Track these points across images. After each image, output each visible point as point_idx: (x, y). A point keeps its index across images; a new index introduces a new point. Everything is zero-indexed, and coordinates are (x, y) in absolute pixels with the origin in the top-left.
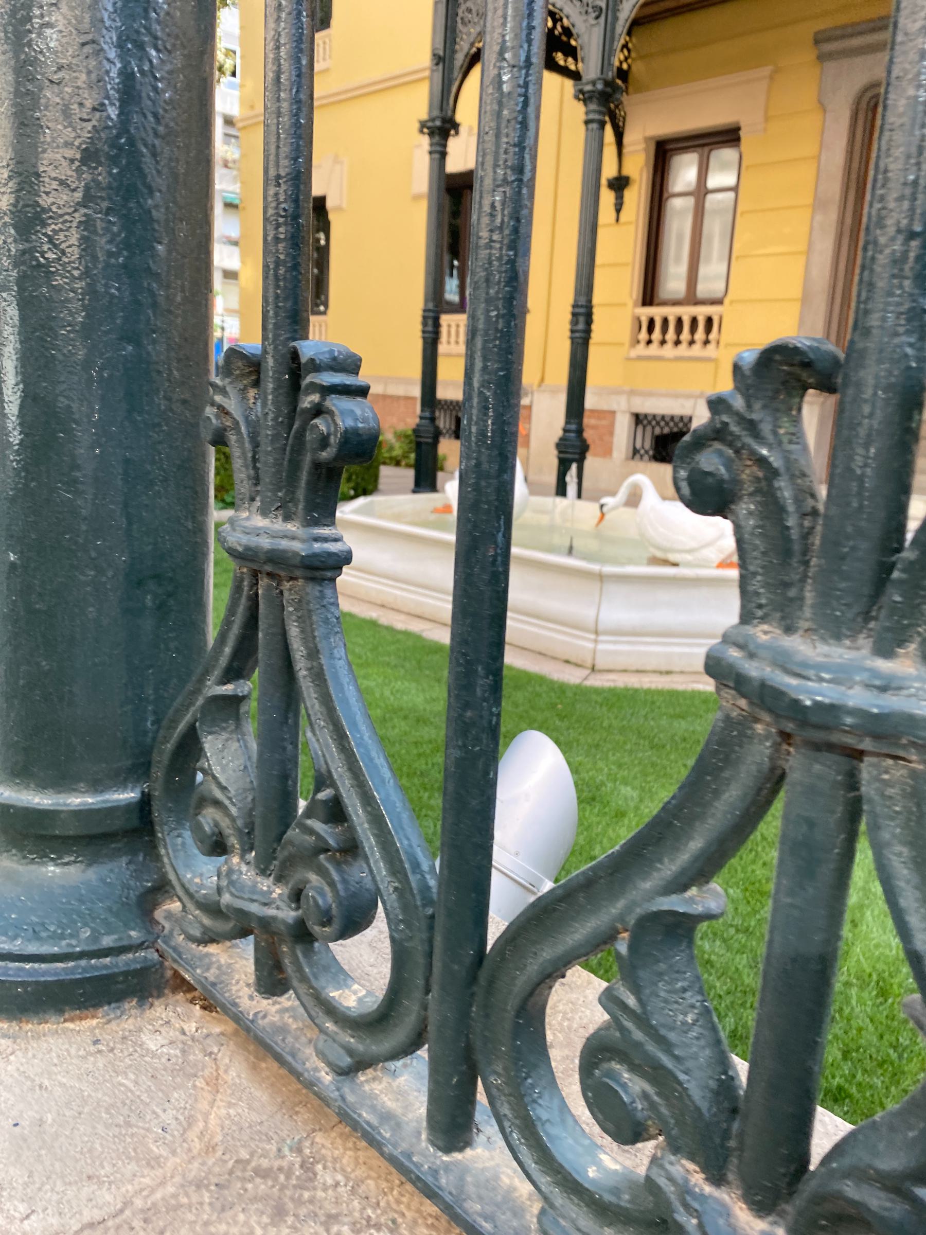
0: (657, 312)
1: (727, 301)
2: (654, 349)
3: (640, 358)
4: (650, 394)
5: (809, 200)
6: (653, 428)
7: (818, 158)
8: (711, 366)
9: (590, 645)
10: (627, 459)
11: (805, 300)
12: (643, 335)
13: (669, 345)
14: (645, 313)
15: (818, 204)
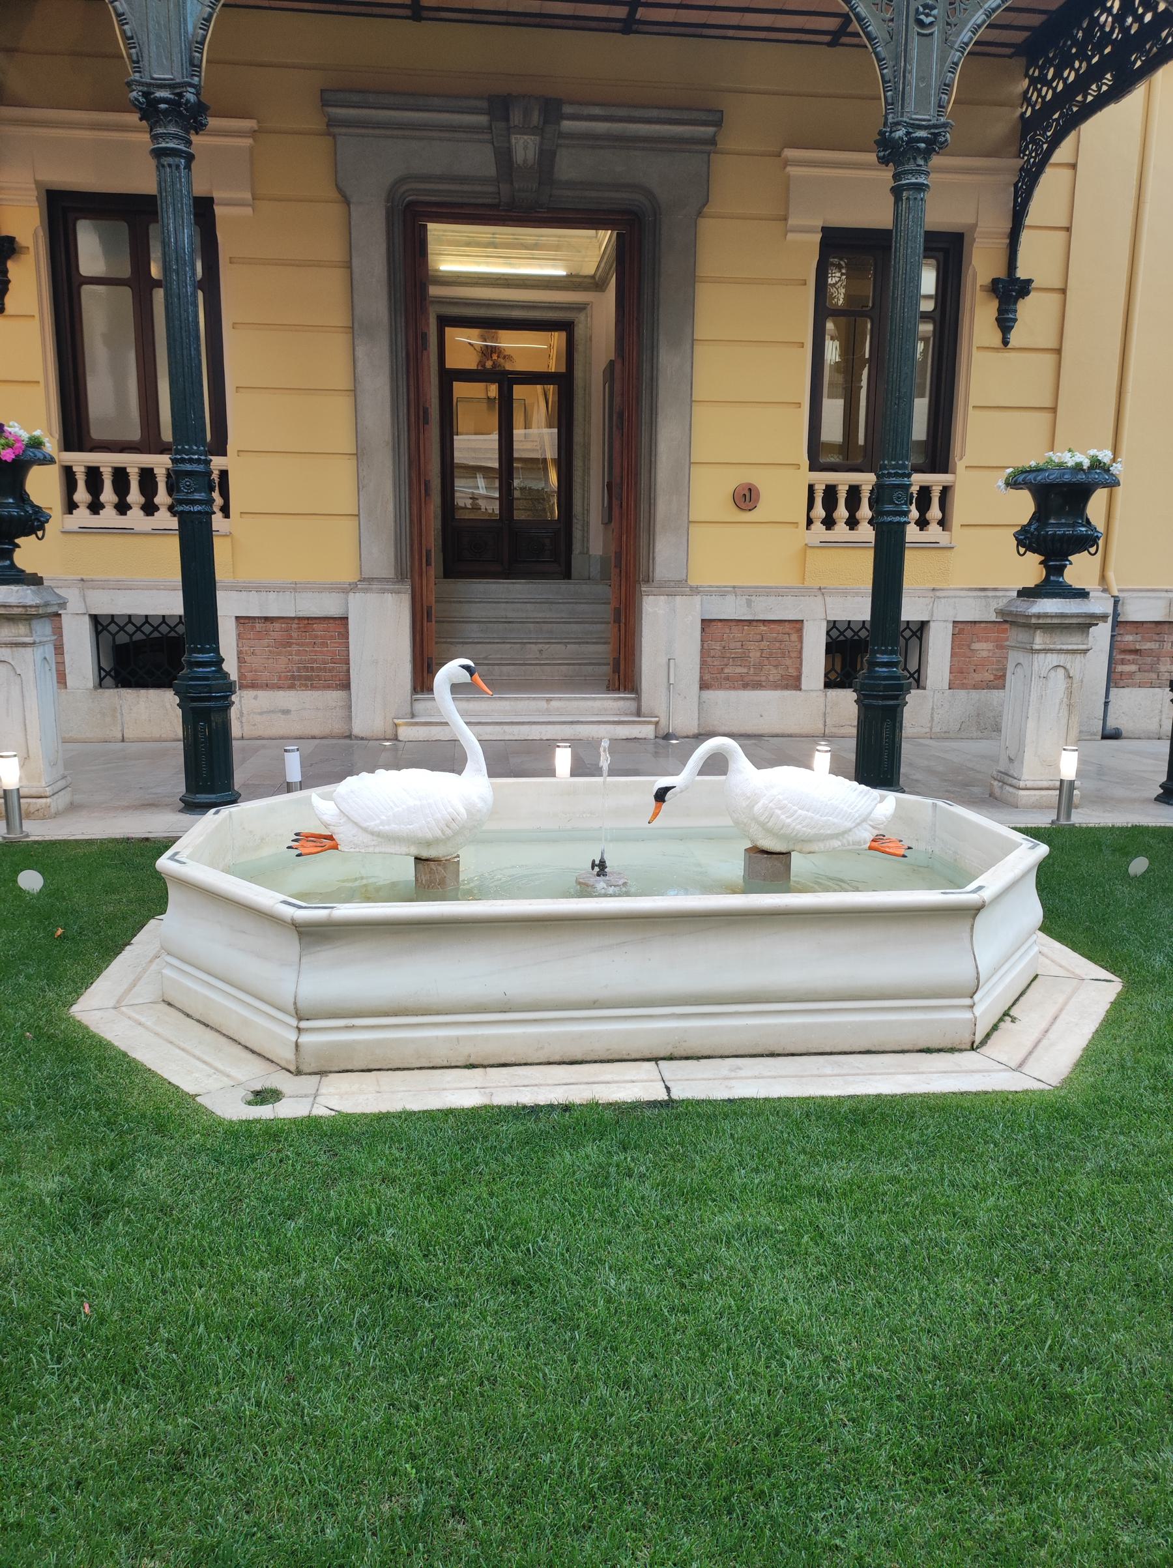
0: (106, 461)
1: (230, 448)
2: (108, 516)
3: (85, 530)
4: (120, 586)
5: (339, 318)
6: (114, 635)
7: (349, 265)
8: (228, 540)
9: (967, 1015)
10: (95, 688)
11: (360, 454)
12: (82, 495)
13: (136, 514)
14: (80, 460)
15: (355, 329)
